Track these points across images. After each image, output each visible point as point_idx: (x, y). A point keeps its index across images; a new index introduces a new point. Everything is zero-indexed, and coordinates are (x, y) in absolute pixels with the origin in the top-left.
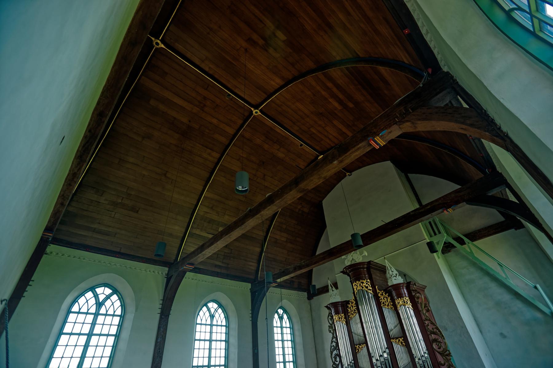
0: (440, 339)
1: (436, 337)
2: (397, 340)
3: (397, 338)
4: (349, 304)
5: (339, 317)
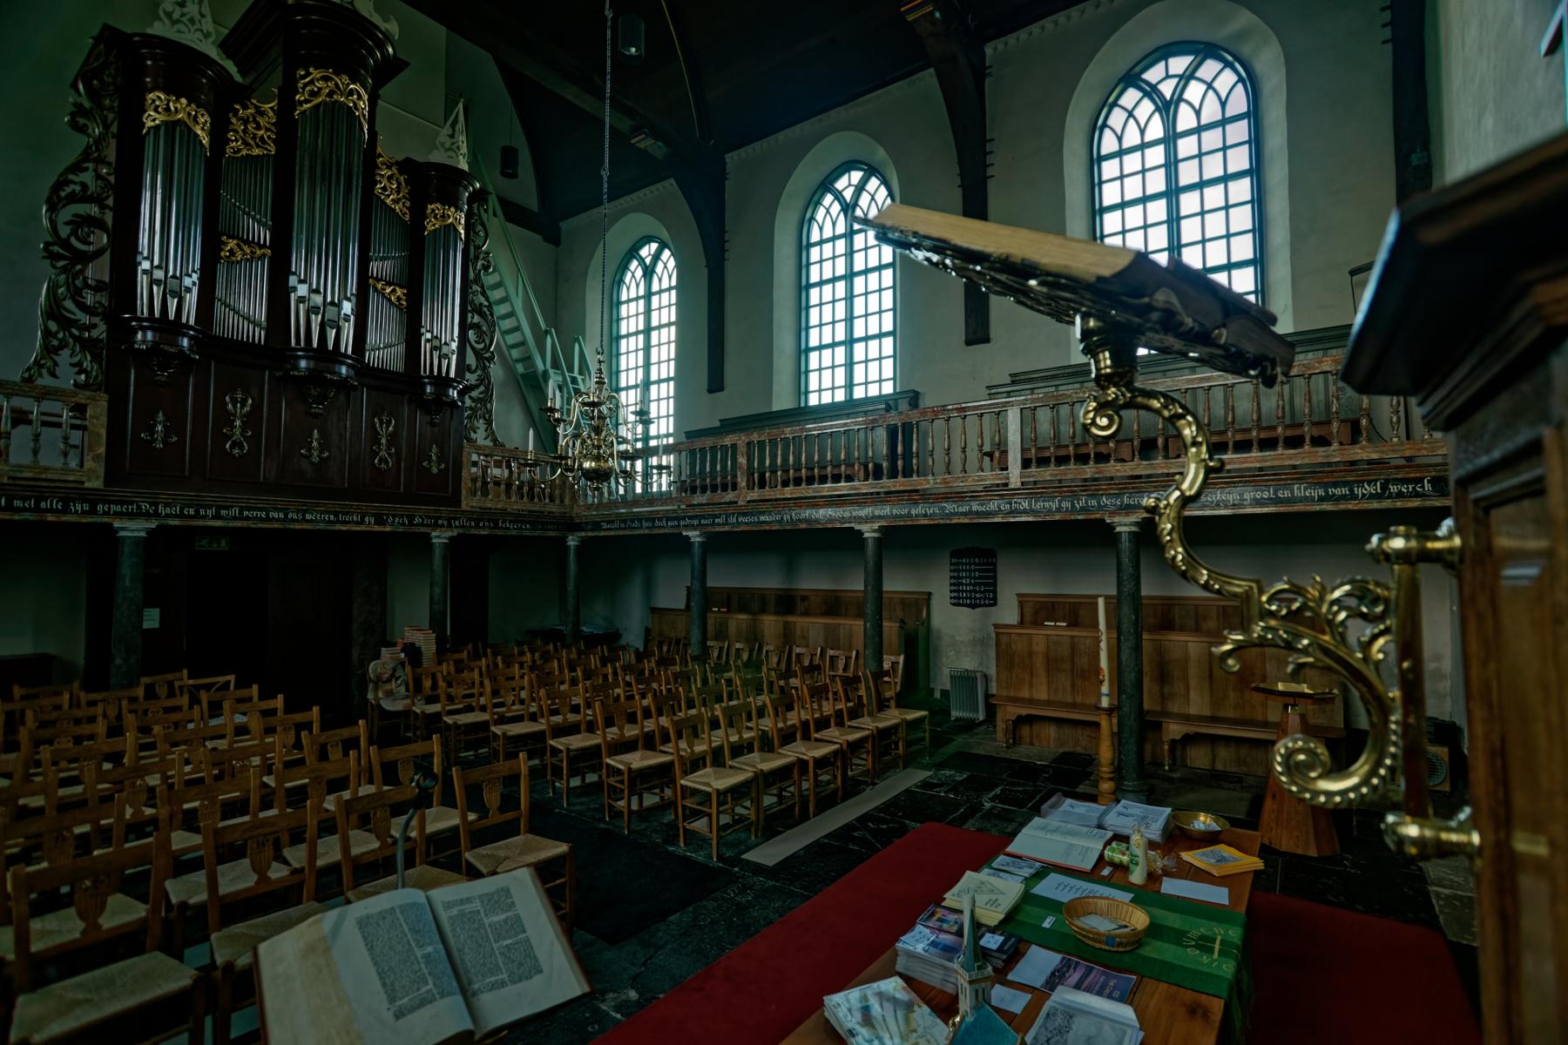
1: (483, 322)
3: (389, 284)
4: (245, 107)
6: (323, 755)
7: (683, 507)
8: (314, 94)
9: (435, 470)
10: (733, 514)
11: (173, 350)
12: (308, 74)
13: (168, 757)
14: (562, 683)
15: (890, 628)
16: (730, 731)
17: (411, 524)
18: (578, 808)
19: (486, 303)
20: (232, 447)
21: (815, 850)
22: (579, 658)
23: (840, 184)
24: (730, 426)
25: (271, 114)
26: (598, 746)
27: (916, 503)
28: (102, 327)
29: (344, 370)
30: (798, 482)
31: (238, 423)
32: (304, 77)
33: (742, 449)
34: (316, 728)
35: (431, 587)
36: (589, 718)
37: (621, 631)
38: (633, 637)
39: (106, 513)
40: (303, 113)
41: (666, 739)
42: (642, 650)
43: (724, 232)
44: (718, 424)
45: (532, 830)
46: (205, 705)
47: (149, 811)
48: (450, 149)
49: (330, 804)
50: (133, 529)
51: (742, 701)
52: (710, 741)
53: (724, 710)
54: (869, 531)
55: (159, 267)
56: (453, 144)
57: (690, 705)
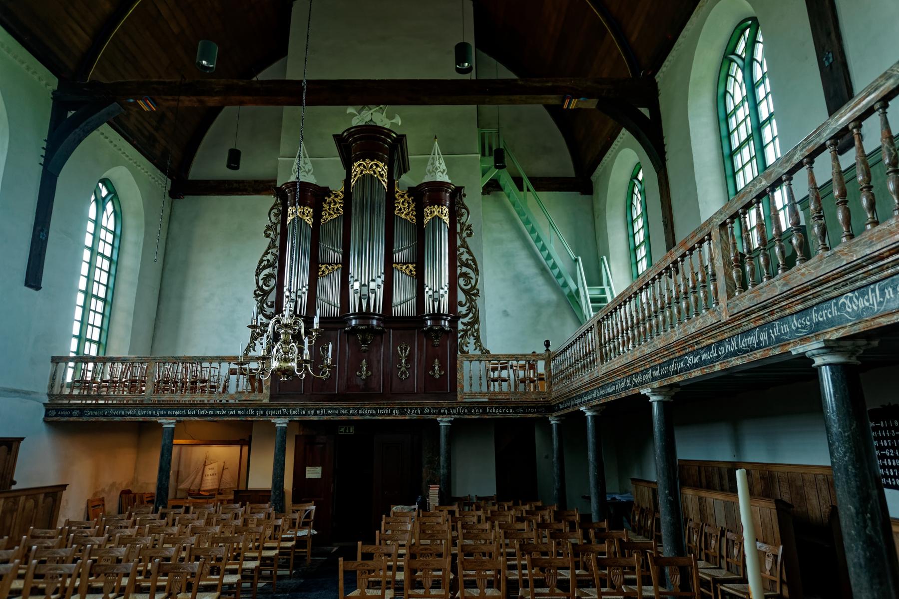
0: (472, 275)
2: (404, 267)
3: (404, 264)
4: (329, 197)
5: (304, 211)
8: (355, 176)
9: (437, 376)
17: (422, 413)
19: (471, 258)
29: (375, 322)
39: (269, 415)
48: (433, 171)
56: (433, 168)
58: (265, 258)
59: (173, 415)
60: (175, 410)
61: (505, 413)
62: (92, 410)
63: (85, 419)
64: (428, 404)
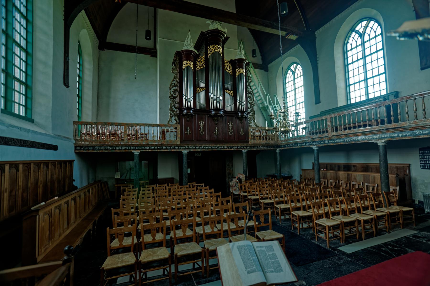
3: (229, 90)
4: (199, 59)
6: (222, 204)
7: (310, 139)
8: (211, 51)
9: (242, 134)
10: (327, 140)
11: (190, 114)
12: (210, 47)
13: (194, 201)
14: (277, 189)
15: (392, 177)
16: (331, 207)
18: (284, 225)
19: (251, 91)
20: (201, 133)
21: (366, 251)
22: (282, 183)
23: (357, 29)
24: (323, 113)
25: (204, 58)
26: (289, 208)
27: (401, 132)
28: (178, 111)
30: (350, 128)
31: (202, 128)
32: (209, 48)
33: (328, 120)
34: (220, 197)
35: (243, 163)
36: (286, 200)
37: (293, 176)
38: (296, 177)
39: (181, 149)
40: (210, 56)
41: (310, 208)
42: (299, 181)
43: (316, 55)
44: (319, 113)
45: (272, 229)
46: (199, 190)
47: (191, 212)
48: (240, 54)
49: (225, 215)
50: (185, 152)
51: (334, 198)
52: (324, 210)
53: (329, 201)
54: (380, 143)
55: (186, 97)
57: (317, 198)
58: (173, 82)
59: (139, 149)
60: (139, 147)
61: (264, 148)
62: (100, 147)
63: (96, 151)
64: (240, 145)
